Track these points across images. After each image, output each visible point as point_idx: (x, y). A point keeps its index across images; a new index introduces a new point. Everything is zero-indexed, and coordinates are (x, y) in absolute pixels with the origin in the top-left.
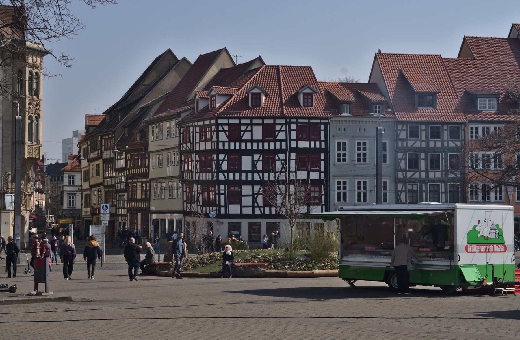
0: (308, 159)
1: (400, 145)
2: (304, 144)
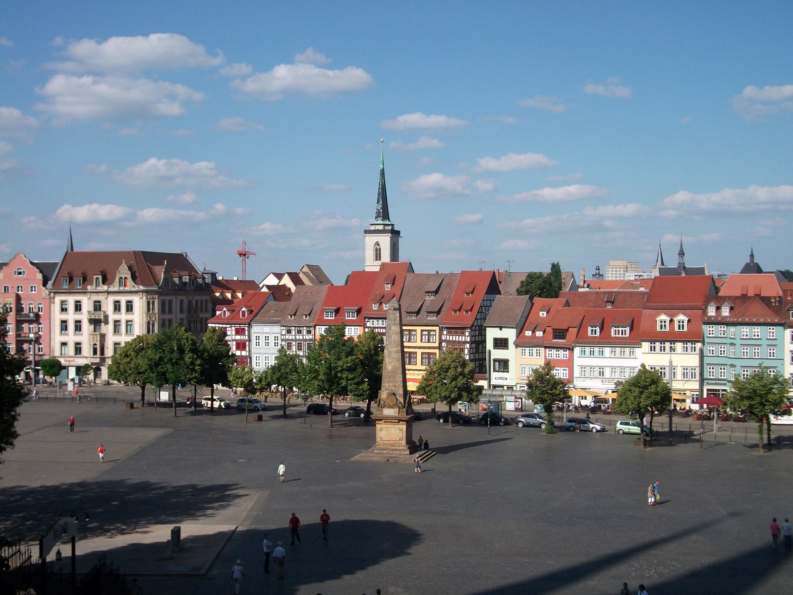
1: (282, 338)
2: (238, 337)
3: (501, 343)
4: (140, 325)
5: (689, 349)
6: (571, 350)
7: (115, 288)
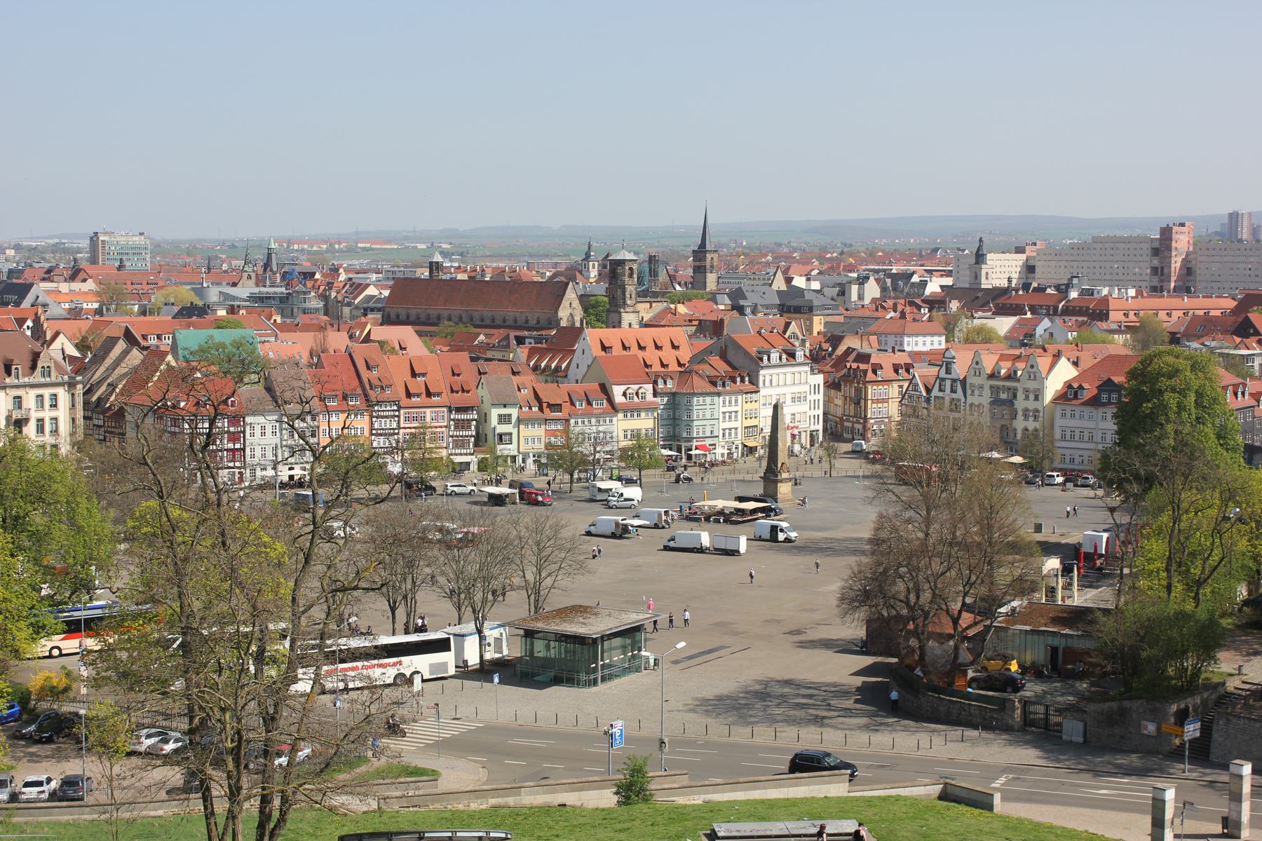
0: (234, 438)
2: (232, 429)
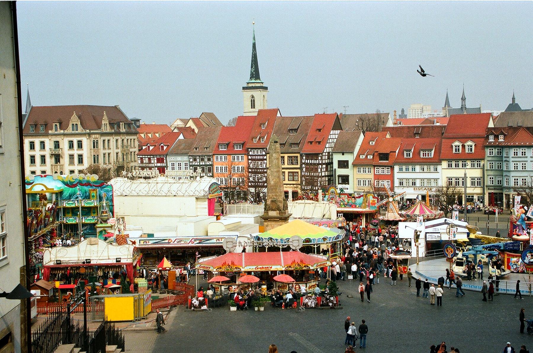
2: (159, 165)
3: (343, 164)
4: (88, 158)
5: (476, 165)
6: (392, 168)
7: (70, 130)
